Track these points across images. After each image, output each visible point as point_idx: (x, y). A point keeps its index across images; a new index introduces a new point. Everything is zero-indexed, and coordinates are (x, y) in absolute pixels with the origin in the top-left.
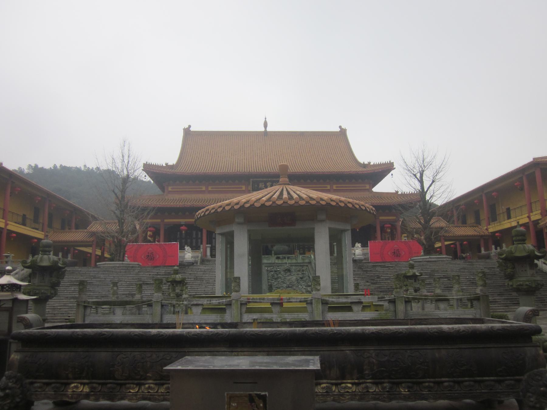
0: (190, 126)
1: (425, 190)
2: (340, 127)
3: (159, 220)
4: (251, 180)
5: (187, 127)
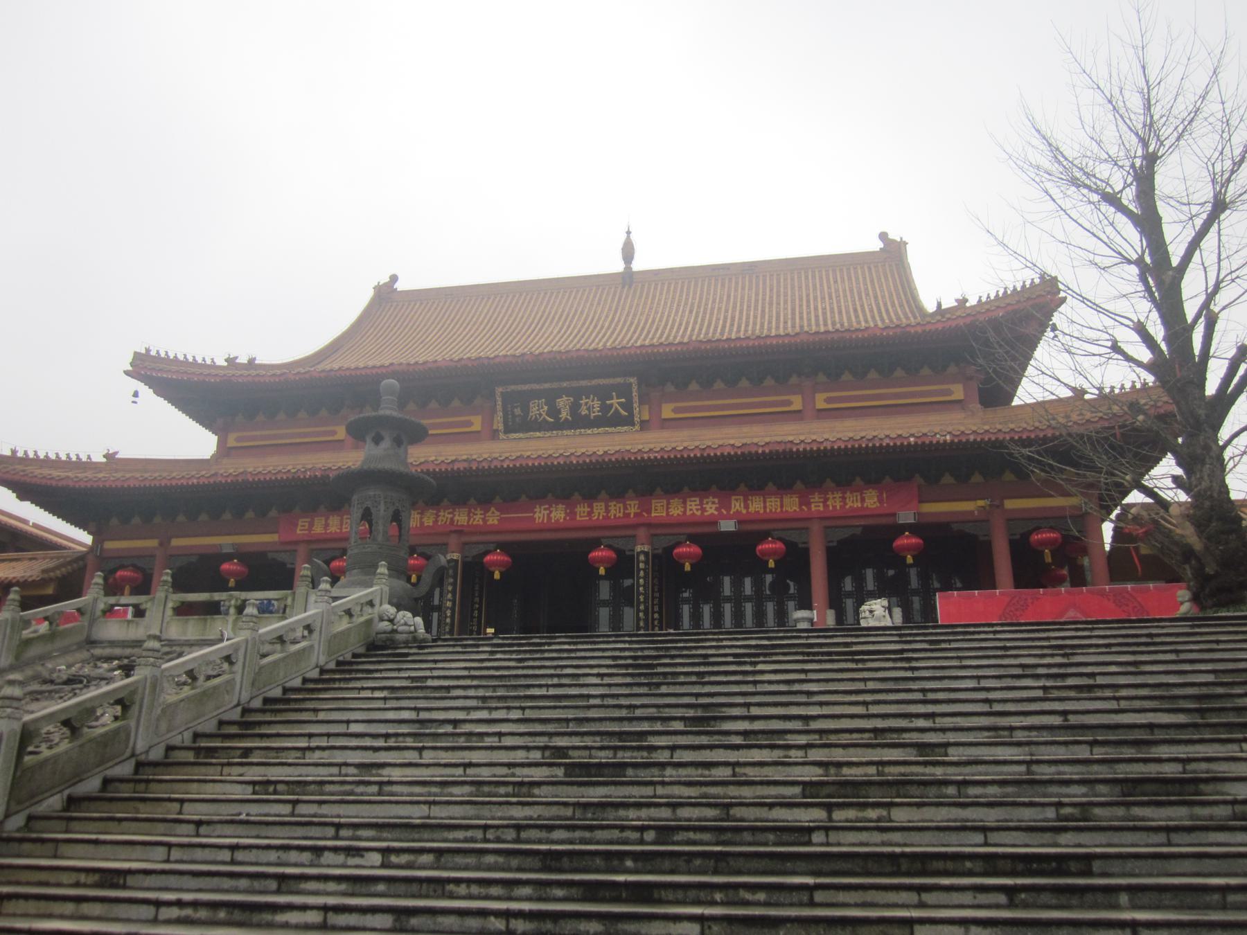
0: (394, 278)
1: (1175, 261)
2: (883, 236)
3: (153, 543)
4: (499, 390)
5: (385, 279)
